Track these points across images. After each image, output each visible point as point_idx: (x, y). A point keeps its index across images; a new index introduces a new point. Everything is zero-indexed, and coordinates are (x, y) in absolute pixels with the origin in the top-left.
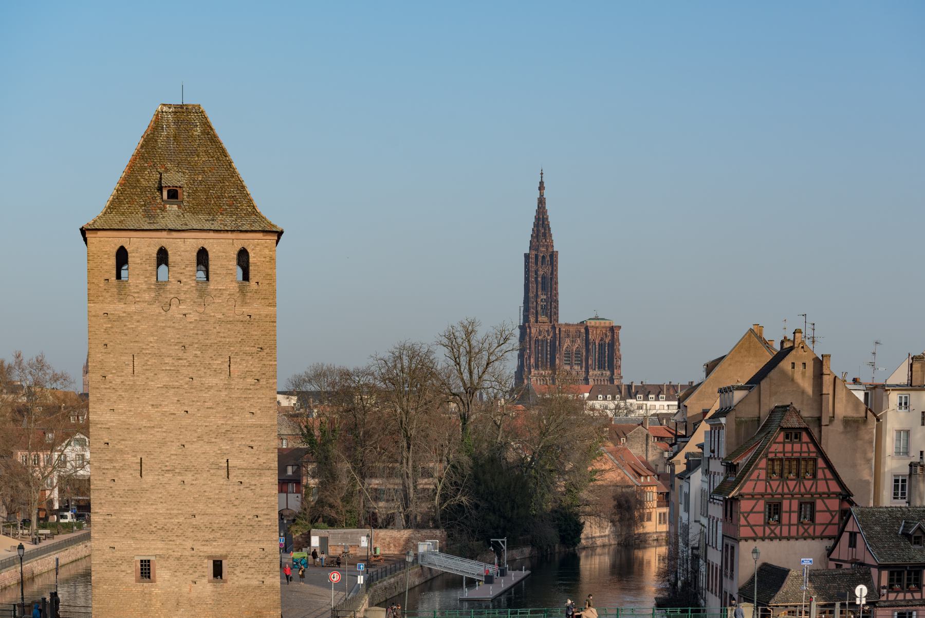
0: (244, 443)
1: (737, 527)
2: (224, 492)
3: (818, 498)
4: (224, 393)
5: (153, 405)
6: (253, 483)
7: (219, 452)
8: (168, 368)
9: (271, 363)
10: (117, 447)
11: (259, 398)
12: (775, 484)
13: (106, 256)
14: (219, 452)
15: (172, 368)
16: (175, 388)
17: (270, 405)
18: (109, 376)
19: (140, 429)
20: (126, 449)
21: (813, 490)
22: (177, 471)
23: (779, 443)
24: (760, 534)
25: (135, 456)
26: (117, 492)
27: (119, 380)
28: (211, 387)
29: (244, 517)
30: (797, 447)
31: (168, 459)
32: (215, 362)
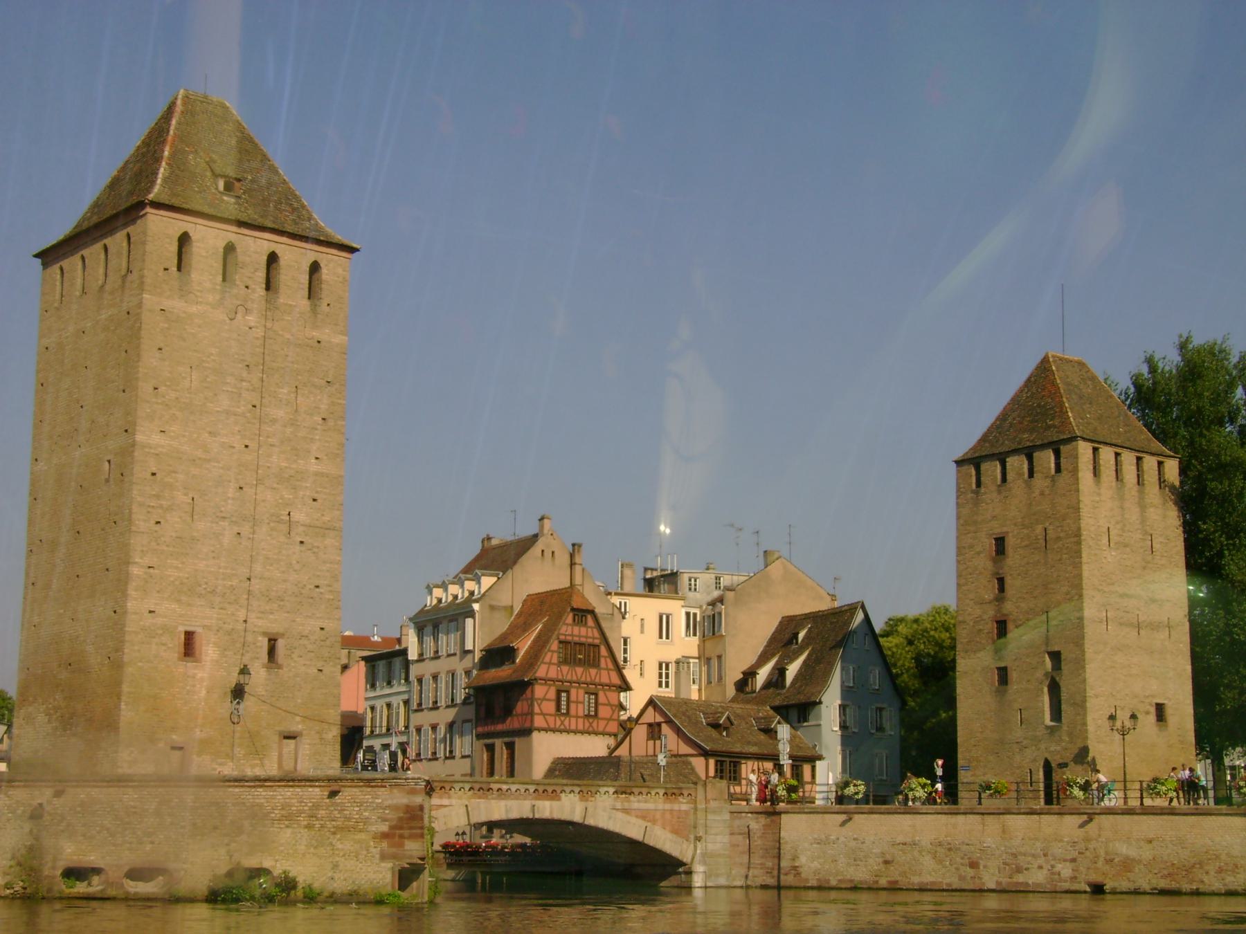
0: (308, 494)
1: (531, 713)
2: (284, 552)
3: (600, 689)
4: (289, 430)
5: (210, 433)
6: (316, 544)
7: (280, 501)
8: (230, 389)
9: (339, 401)
10: (167, 480)
11: (327, 441)
12: (565, 668)
13: (168, 240)
14: (280, 501)
15: (234, 390)
16: (235, 415)
17: (337, 452)
18: (162, 389)
19: (194, 460)
20: (177, 484)
21: (597, 680)
22: (234, 519)
23: (567, 624)
24: (552, 726)
25: (186, 495)
26: (162, 539)
27: (173, 395)
28: (274, 421)
29: (305, 586)
30: (583, 630)
31: (223, 503)
32: (281, 390)
